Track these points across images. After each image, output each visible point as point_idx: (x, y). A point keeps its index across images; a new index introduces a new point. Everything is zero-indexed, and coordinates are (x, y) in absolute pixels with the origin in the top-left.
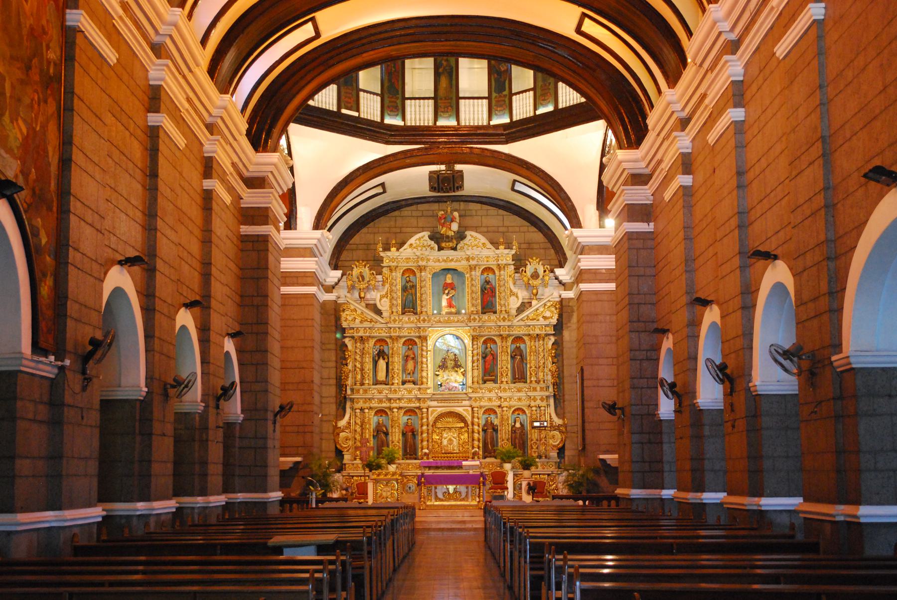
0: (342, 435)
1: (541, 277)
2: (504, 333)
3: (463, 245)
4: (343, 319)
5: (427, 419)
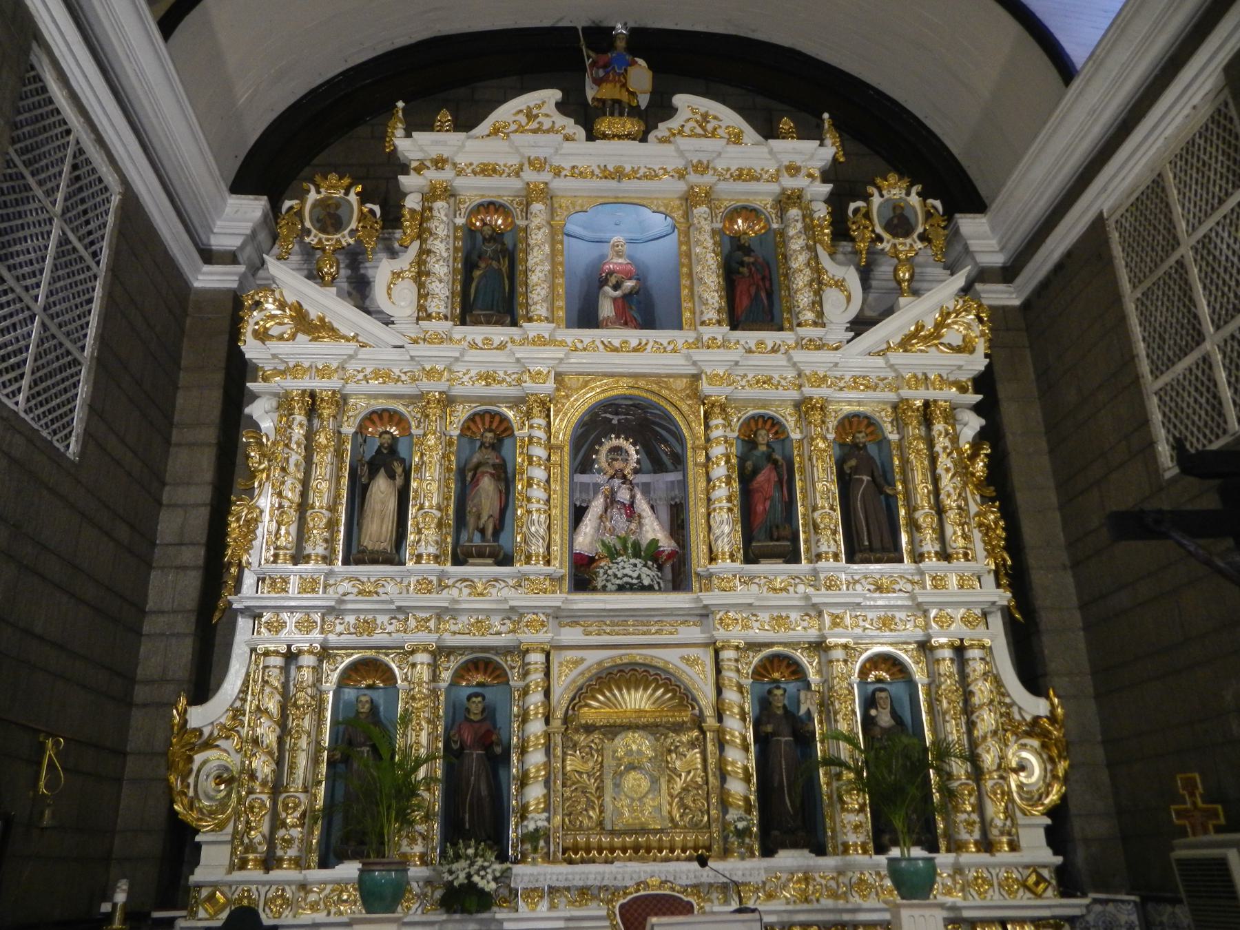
0: (210, 760)
1: (920, 229)
2: (816, 393)
3: (667, 134)
4: (248, 330)
5: (547, 693)
